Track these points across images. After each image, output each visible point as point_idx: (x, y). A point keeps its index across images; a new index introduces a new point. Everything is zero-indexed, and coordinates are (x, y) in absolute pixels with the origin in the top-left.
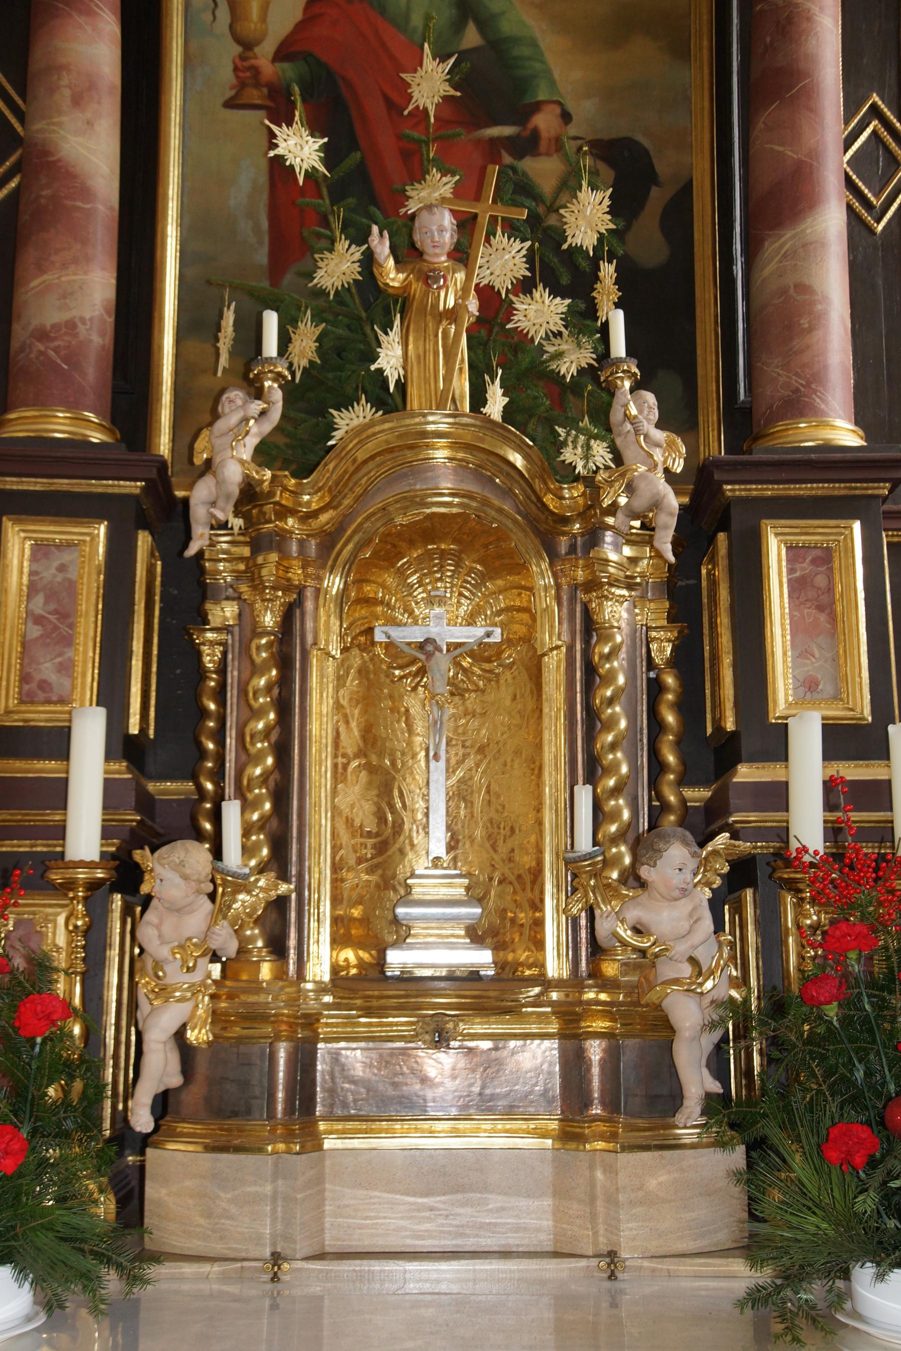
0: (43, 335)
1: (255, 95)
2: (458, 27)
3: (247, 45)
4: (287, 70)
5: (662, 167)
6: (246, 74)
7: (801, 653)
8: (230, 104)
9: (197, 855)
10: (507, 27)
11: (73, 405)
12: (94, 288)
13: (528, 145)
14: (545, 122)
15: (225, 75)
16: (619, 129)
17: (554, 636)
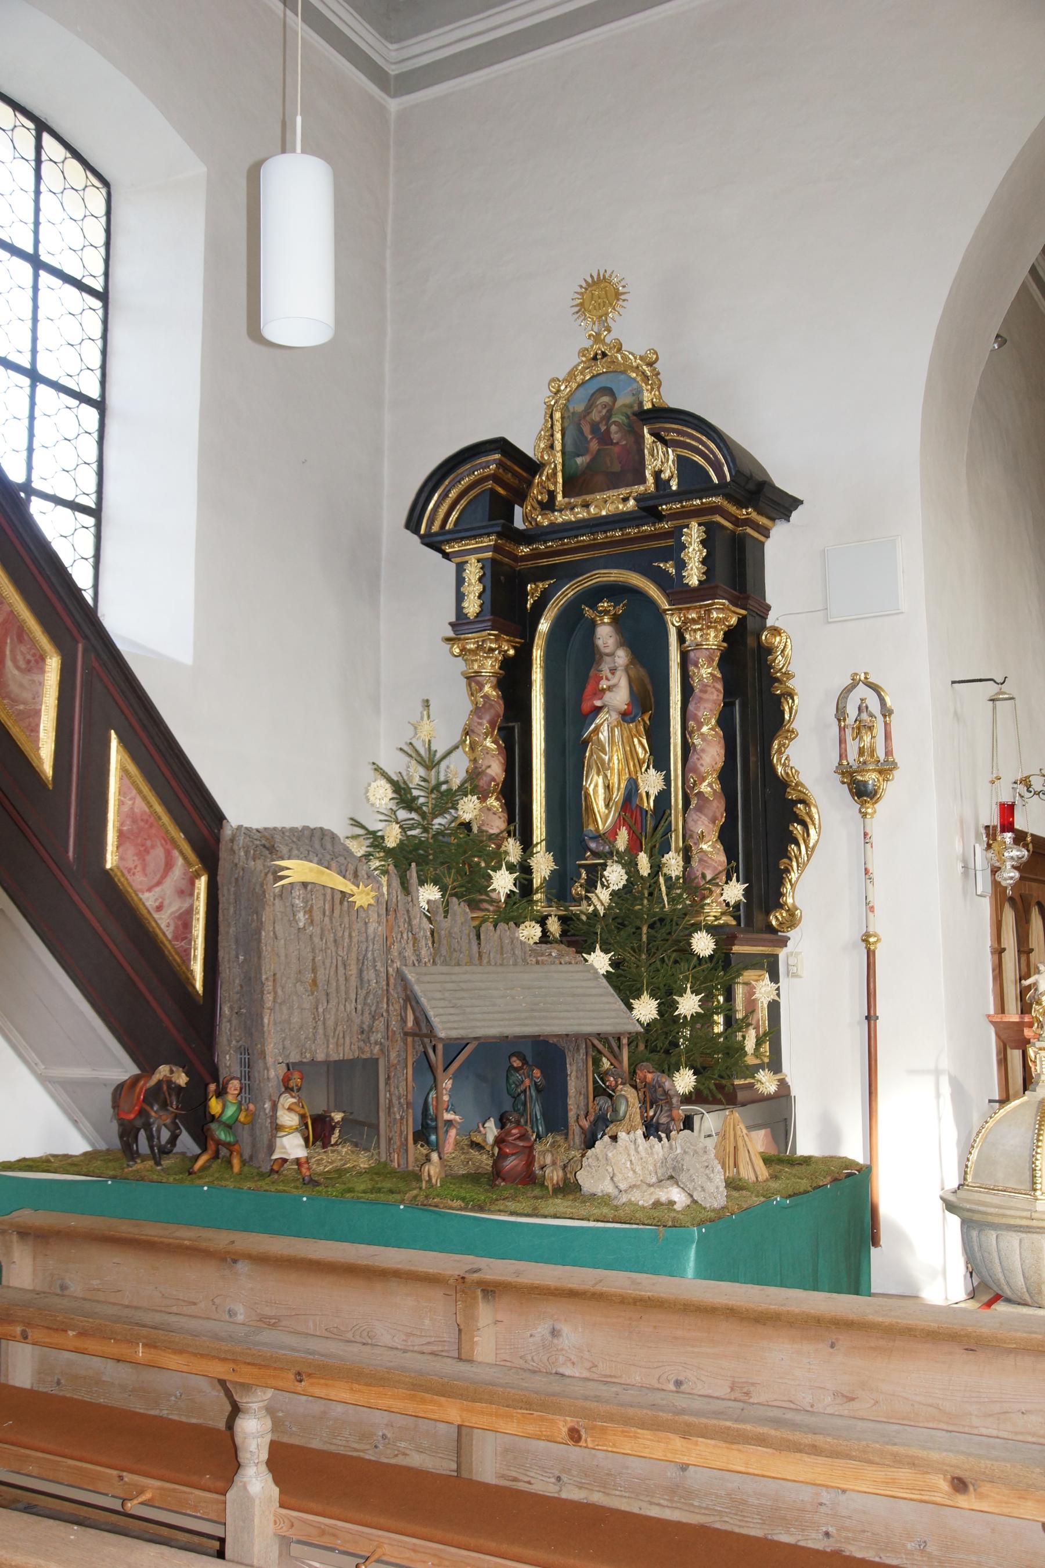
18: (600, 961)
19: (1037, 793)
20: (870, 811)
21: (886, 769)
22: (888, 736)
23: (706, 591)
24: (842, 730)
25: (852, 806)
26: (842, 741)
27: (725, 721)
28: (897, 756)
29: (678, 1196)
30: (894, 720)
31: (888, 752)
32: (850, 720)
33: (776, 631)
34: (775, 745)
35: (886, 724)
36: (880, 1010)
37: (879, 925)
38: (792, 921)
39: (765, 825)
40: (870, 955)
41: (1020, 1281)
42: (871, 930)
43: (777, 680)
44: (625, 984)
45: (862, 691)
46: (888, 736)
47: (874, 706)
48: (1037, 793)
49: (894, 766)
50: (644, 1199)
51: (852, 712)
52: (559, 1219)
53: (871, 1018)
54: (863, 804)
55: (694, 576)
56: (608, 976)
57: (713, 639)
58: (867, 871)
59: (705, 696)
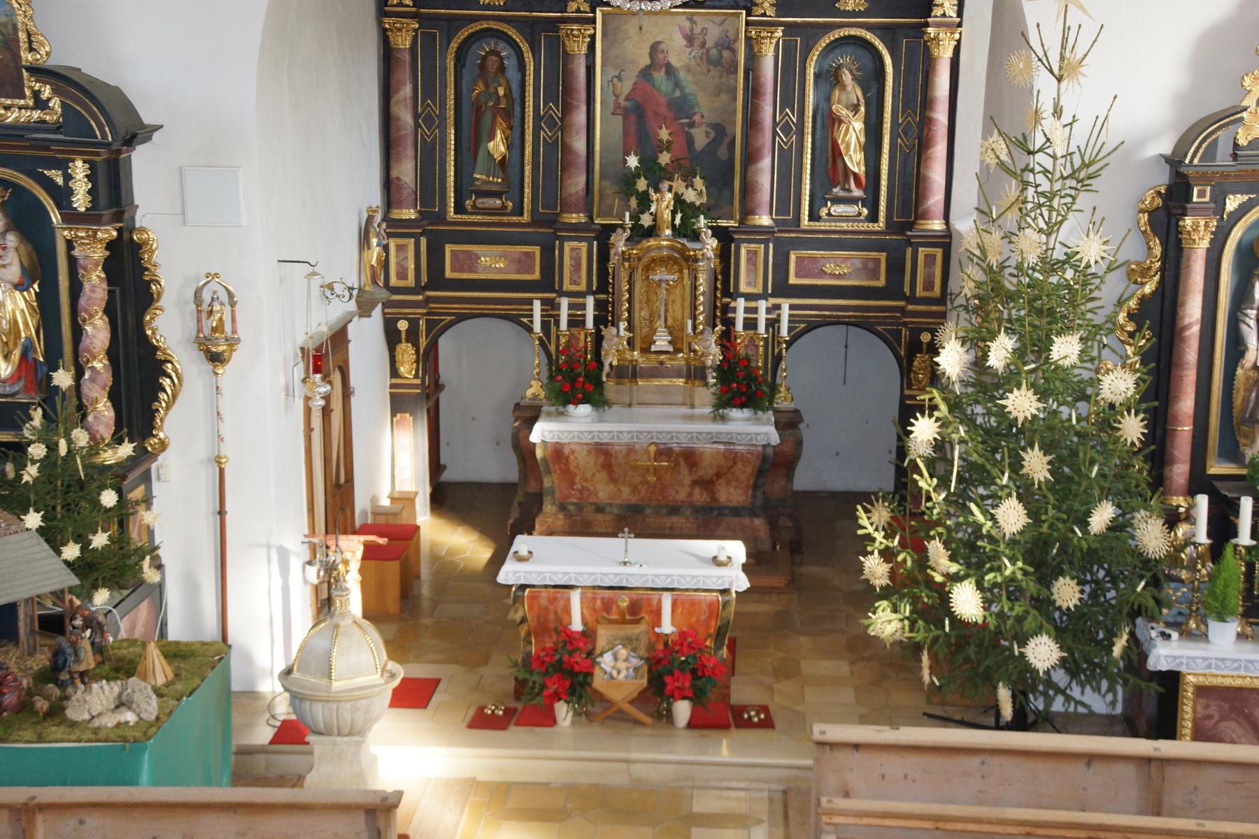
0: (570, 195)
1: (619, 111)
2: (674, 90)
3: (617, 96)
4: (628, 104)
5: (728, 131)
6: (617, 105)
7: (748, 276)
8: (613, 114)
9: (614, 330)
10: (687, 90)
11: (578, 212)
12: (582, 179)
13: (692, 125)
14: (697, 118)
15: (611, 106)
16: (718, 120)
17: (687, 282)
18: (33, 520)
19: (338, 296)
20: (220, 371)
21: (233, 343)
22: (233, 320)
23: (90, 218)
24: (199, 312)
25: (209, 367)
26: (199, 320)
27: (109, 311)
28: (241, 333)
29: (130, 717)
30: (237, 308)
31: (234, 332)
32: (205, 307)
33: (142, 230)
34: (149, 332)
35: (233, 312)
36: (229, 507)
37: (227, 450)
38: (163, 445)
39: (140, 384)
40: (222, 471)
41: (321, 725)
42: (222, 454)
43: (147, 269)
44: (52, 536)
45: (213, 286)
46: (233, 320)
47: (224, 297)
48: (338, 296)
49: (238, 340)
50: (109, 721)
51: (207, 296)
52: (59, 742)
53: (222, 512)
54: (215, 367)
55: (81, 201)
56: (40, 530)
57: (99, 254)
58: (218, 414)
59: (94, 295)
